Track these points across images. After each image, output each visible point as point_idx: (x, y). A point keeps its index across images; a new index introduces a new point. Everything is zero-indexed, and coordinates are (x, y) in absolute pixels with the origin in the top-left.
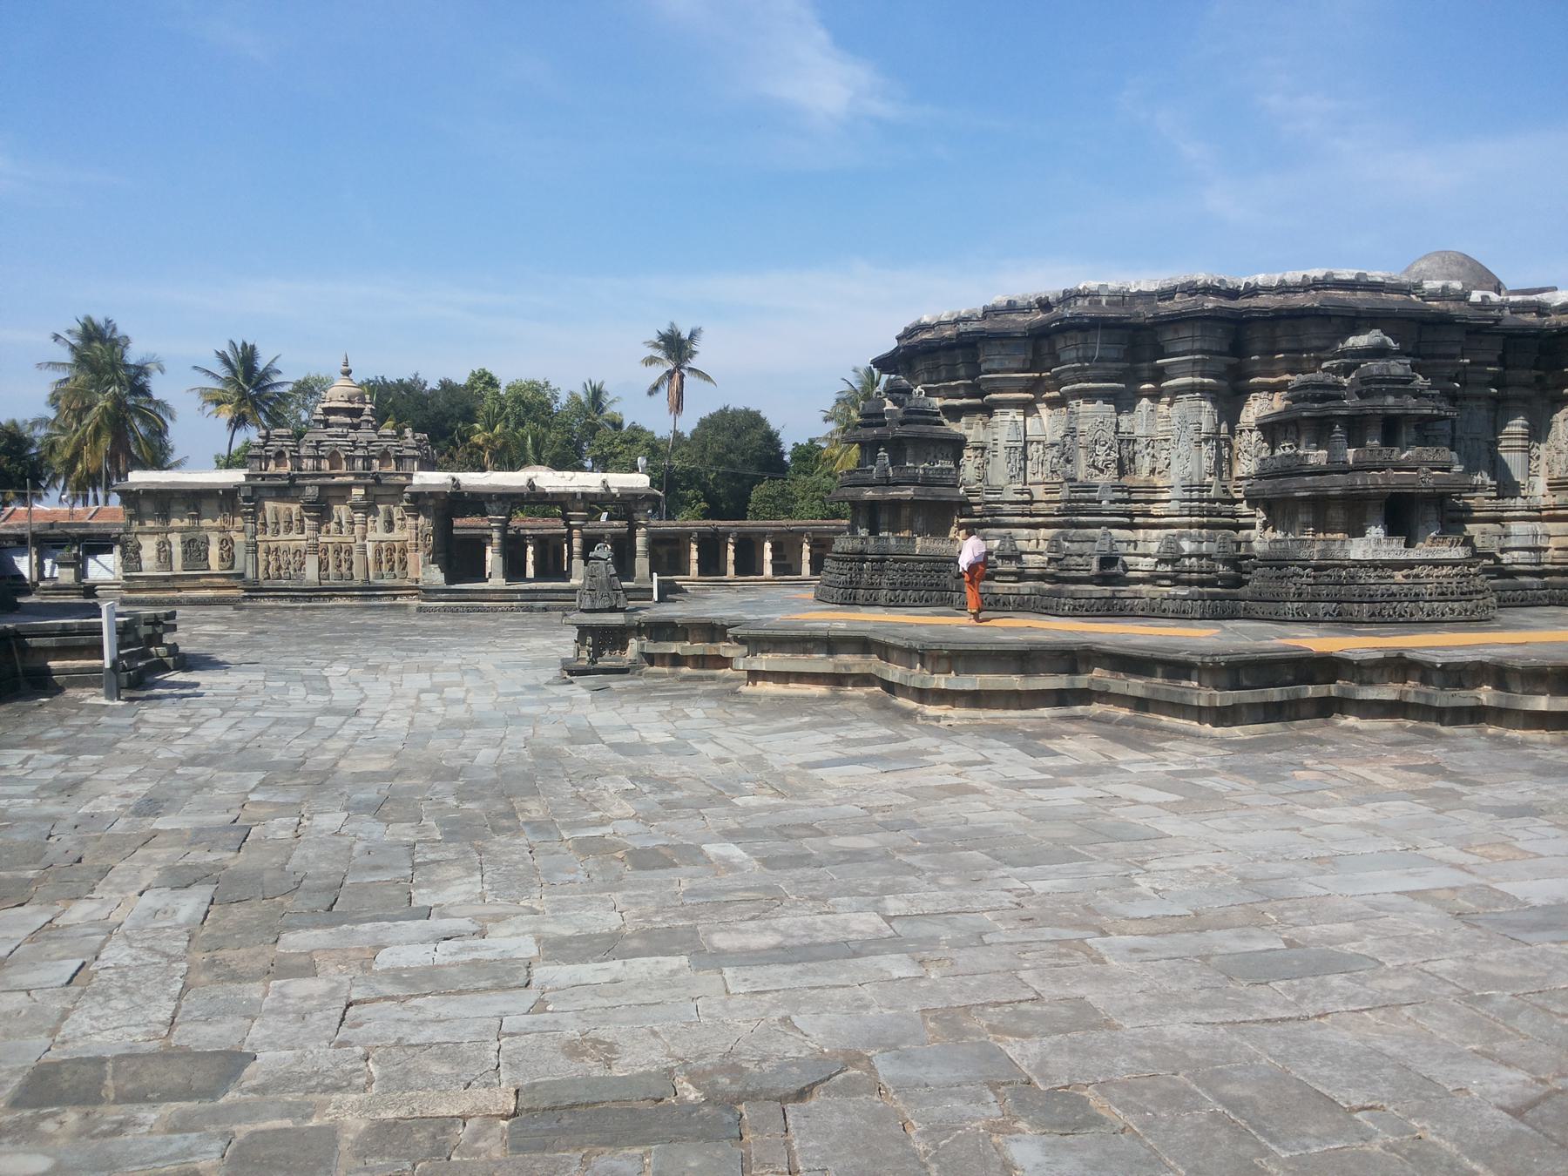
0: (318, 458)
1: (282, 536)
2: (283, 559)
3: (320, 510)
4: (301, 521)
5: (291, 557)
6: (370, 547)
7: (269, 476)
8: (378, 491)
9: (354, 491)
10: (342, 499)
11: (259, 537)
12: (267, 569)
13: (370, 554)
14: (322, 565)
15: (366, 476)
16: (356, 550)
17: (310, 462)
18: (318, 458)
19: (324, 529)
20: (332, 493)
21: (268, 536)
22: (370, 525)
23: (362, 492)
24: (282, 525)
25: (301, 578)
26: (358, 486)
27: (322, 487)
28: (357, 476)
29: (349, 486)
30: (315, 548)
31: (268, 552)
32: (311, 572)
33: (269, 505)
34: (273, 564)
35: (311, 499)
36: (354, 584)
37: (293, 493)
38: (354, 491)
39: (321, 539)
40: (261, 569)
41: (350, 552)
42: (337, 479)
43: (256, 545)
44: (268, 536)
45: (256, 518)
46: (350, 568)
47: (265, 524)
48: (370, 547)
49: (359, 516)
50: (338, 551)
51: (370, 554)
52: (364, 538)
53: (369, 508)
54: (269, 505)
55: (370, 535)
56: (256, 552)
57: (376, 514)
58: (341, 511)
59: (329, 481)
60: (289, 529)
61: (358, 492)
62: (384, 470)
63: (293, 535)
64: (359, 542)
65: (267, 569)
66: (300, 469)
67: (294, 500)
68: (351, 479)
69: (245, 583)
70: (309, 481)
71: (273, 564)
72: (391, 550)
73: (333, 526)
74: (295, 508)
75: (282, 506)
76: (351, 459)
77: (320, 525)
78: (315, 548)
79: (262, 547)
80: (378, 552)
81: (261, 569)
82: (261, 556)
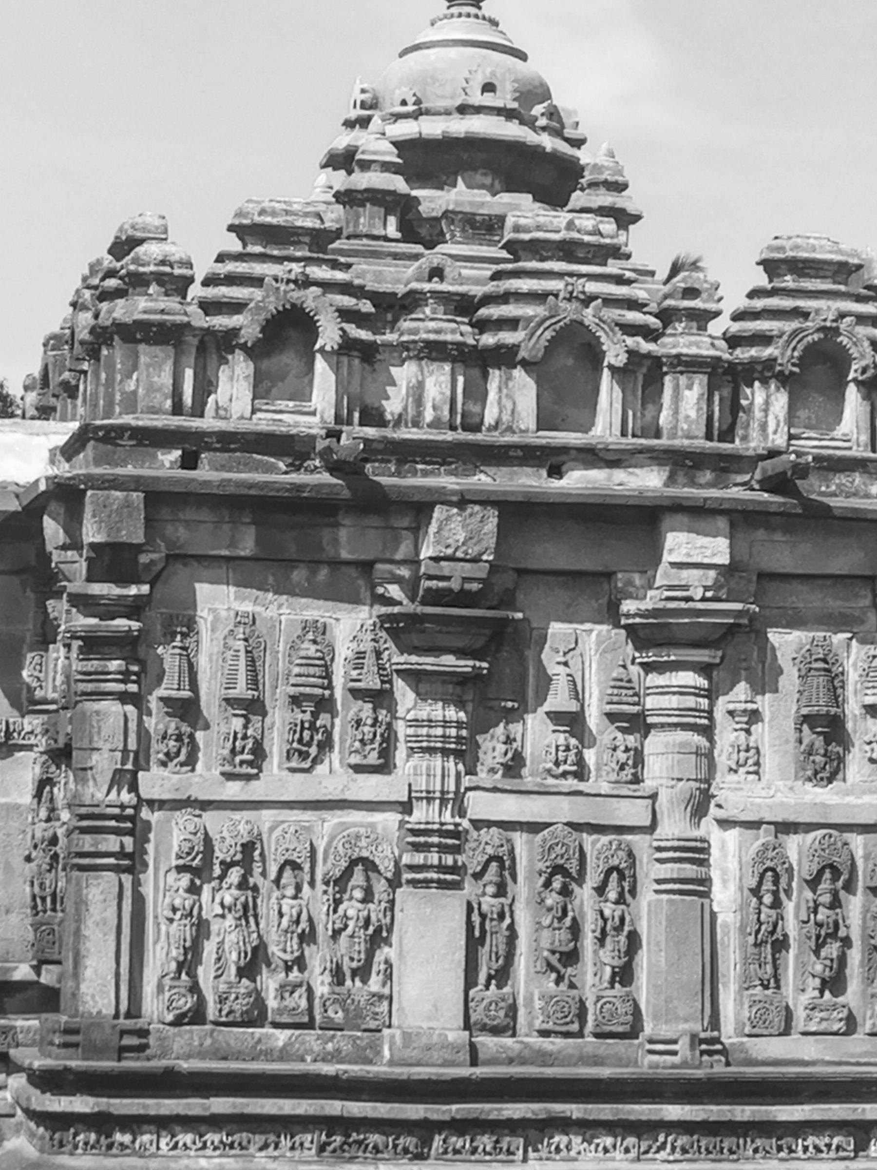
0: (476, 362)
1: (277, 779)
2: (276, 909)
3: (478, 647)
4: (381, 698)
5: (317, 901)
6: (730, 859)
7: (228, 441)
8: (781, 554)
9: (679, 543)
10: (595, 592)
11: (156, 782)
12: (189, 962)
13: (726, 897)
14: (484, 951)
15: (726, 465)
16: (650, 870)
17: (439, 383)
18: (476, 362)
19: (492, 749)
20: (552, 553)
21: (206, 779)
22: (727, 736)
23: (716, 549)
24: (280, 720)
25: (365, 1022)
26: (698, 514)
27: (517, 513)
28: (682, 463)
29: (639, 524)
30: (444, 856)
31: (199, 868)
32: (424, 991)
33: (217, 603)
34: (227, 939)
35: (457, 575)
36: (647, 1064)
37: (348, 541)
38: (679, 543)
39: (481, 806)
40: (160, 957)
41: (623, 877)
42: (577, 481)
43: (139, 831)
44: (206, 779)
45: (147, 672)
46: (624, 975)
47: (187, 710)
48: (730, 859)
49: (672, 689)
50: (563, 875)
51: (726, 897)
52: (700, 804)
53: (728, 648)
54: (217, 603)
55: (734, 793)
56: (132, 863)
57: (765, 679)
58: (582, 656)
59: (531, 481)
60: (310, 747)
61: (692, 554)
62: (811, 444)
63: (332, 778)
64: (674, 826)
65: (189, 962)
66: (373, 416)
67: (351, 581)
68: (649, 480)
69: (73, 1036)
70: (447, 481)
71: (227, 939)
72: (835, 875)
73: (537, 734)
74: (350, 626)
75: (283, 613)
76: (646, 376)
77: (480, 725)
78: (444, 856)
79: (172, 835)
80: (769, 881)
81: (160, 957)
82: (162, 887)
